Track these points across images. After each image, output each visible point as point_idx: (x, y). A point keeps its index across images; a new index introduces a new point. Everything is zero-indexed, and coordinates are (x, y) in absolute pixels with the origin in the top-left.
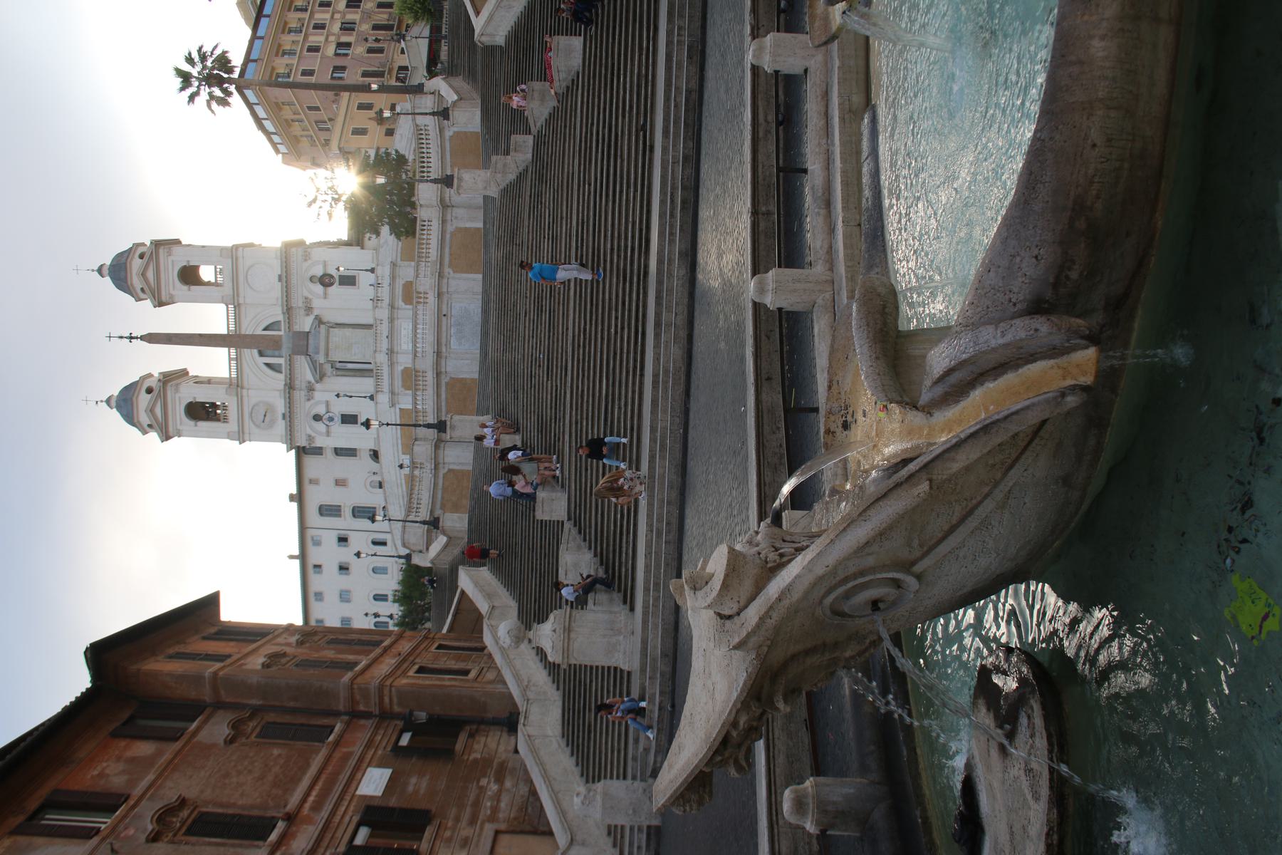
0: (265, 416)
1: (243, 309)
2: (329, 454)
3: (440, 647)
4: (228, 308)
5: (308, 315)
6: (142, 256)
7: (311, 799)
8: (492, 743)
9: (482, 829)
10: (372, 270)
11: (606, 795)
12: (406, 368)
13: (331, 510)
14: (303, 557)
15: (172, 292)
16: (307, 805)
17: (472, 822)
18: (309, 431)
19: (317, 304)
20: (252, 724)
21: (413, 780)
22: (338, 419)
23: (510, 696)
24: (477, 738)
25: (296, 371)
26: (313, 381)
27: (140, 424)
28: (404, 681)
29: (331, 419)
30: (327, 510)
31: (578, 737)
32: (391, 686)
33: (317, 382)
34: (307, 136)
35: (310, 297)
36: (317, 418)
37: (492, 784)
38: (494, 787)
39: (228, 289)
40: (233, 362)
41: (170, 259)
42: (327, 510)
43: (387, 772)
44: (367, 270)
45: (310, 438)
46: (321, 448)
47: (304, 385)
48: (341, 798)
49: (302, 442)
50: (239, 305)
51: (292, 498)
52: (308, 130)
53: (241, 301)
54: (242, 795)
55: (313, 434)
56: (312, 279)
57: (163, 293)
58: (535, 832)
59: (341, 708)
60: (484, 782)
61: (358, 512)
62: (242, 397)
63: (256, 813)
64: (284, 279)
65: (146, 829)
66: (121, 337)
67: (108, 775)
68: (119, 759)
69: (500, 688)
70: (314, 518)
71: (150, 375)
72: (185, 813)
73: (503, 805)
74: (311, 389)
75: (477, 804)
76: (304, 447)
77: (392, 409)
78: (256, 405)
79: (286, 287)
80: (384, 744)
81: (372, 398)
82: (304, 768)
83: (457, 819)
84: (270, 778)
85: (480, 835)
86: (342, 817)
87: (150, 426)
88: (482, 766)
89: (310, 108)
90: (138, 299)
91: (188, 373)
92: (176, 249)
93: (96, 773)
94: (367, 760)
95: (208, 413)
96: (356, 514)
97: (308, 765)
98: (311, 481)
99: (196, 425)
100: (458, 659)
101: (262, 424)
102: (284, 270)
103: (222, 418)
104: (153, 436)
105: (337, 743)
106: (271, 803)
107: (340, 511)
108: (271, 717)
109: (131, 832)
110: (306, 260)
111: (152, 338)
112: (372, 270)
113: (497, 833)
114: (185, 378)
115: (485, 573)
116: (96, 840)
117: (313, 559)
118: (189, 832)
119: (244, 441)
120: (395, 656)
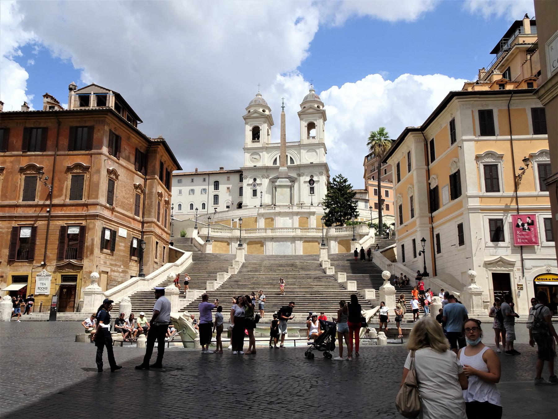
1: (298, 148)
2: (240, 185)
3: (164, 247)
5: (297, 175)
6: (318, 107)
7: (118, 214)
8: (134, 268)
9: (109, 267)
10: (312, 204)
11: (128, 305)
14: (197, 174)
16: (116, 213)
17: (111, 265)
20: (140, 191)
21: (123, 245)
23: (149, 274)
24: (135, 263)
27: (249, 108)
28: (154, 238)
29: (254, 185)
31: (138, 297)
32: (152, 235)
33: (270, 180)
34: (375, 169)
36: (255, 180)
37: (121, 269)
38: (121, 270)
39: (305, 141)
40: (276, 145)
41: (318, 118)
42: (217, 184)
43: (126, 237)
44: (312, 202)
45: (246, 178)
46: (242, 181)
48: (118, 223)
49: (244, 174)
50: (300, 147)
51: (221, 168)
54: (119, 193)
57: (304, 116)
58: (107, 284)
59: (145, 219)
60: (122, 267)
61: (216, 197)
63: (115, 198)
65: (110, 167)
66: (283, 103)
67: (125, 151)
68: (130, 153)
69: (151, 270)
70: (213, 179)
71: (270, 110)
72: (114, 177)
73: (115, 273)
75: (116, 265)
76: (242, 175)
77: (257, 214)
78: (260, 155)
80: (134, 234)
81: (261, 206)
82: (127, 210)
83: (112, 260)
84: (124, 200)
85: (107, 267)
86: (113, 225)
87: (249, 111)
88: (127, 266)
89: (385, 170)
90: (301, 105)
91: (272, 125)
92: (321, 121)
93: (126, 147)
94: (129, 229)
95: (256, 134)
96: (215, 196)
97: (128, 211)
98: (228, 177)
100: (160, 254)
103: (254, 141)
104: (245, 113)
105: (134, 219)
106: (117, 202)
107: (217, 190)
108: (142, 196)
109: (110, 163)
110: (320, 173)
111: (283, 116)
112: (312, 204)
113: (108, 272)
114: (269, 124)
115: (190, 261)
116: (108, 154)
117: (196, 179)
118: (110, 180)
119: (244, 150)
120: (161, 233)
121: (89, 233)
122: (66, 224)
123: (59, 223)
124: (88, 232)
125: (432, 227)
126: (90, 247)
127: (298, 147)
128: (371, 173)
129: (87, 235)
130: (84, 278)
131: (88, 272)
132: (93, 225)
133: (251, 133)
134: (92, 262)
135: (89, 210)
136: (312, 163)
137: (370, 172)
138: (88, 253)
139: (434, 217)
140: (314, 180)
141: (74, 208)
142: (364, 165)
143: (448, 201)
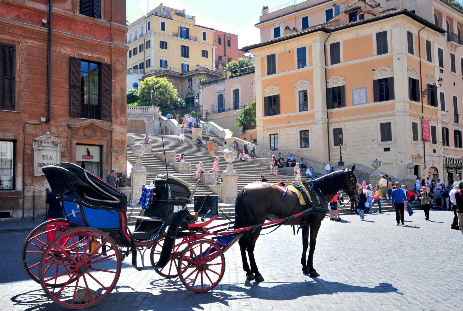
121: (118, 78)
122: (78, 54)
123: (65, 50)
124: (115, 77)
125: (328, 121)
126: (120, 102)
129: (113, 81)
130: (116, 152)
131: (119, 141)
132: (121, 66)
134: (124, 126)
135: (113, 40)
138: (118, 112)
139: (331, 113)
141: (87, 28)
143: (365, 102)
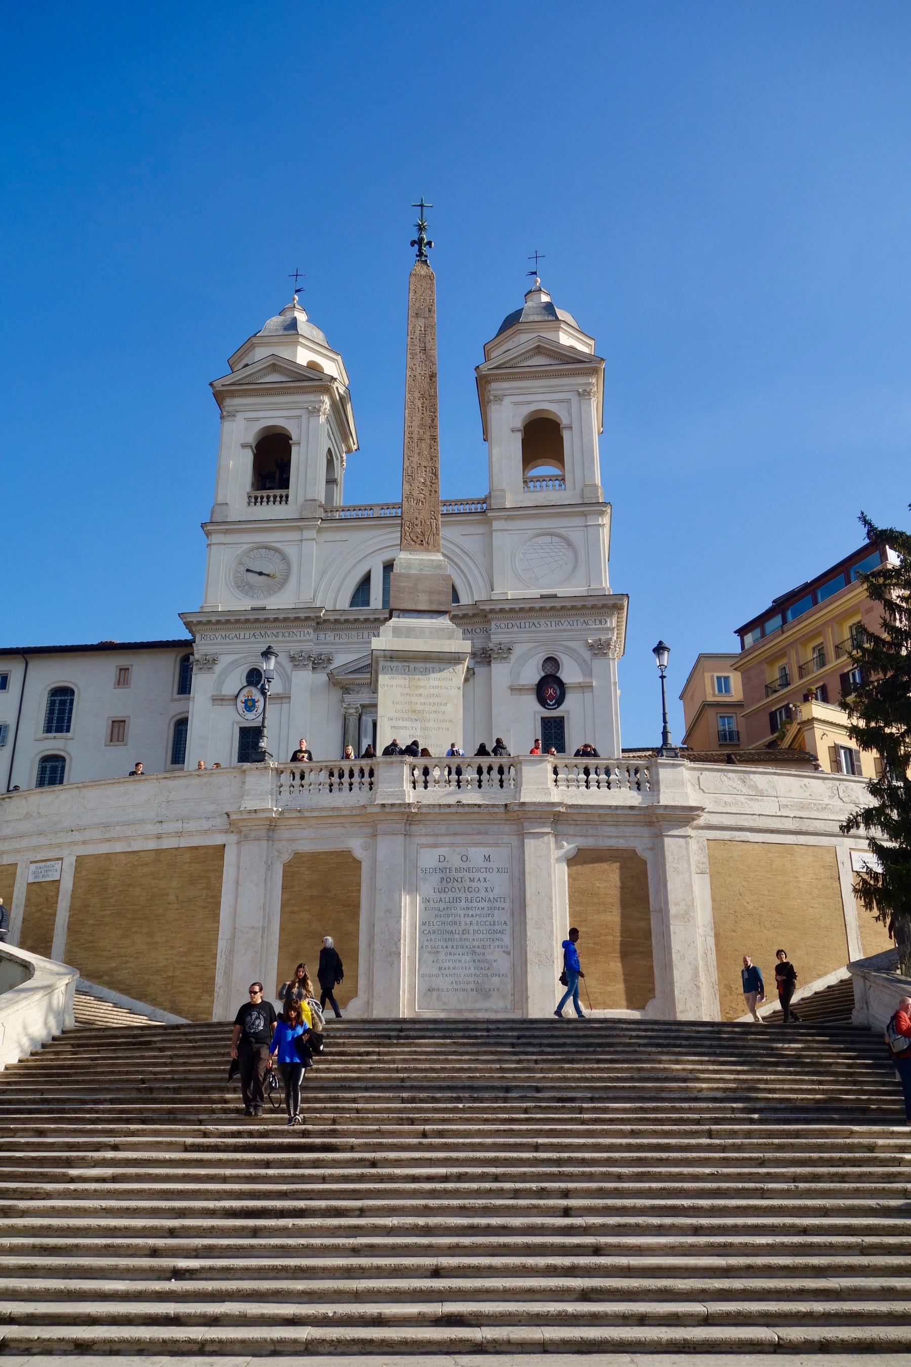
0: (261, 574)
1: (480, 529)
4: (484, 501)
12: (358, 863)
13: (61, 711)
15: (507, 401)
18: (224, 661)
19: (500, 671)
22: (252, 719)
25: (354, 633)
26: (332, 667)
30: (63, 703)
33: (330, 675)
35: (513, 657)
42: (63, 703)
45: (210, 662)
47: (324, 649)
50: (489, 522)
52: (801, 677)
53: (496, 525)
55: (218, 668)
56: (552, 662)
57: (505, 385)
62: (300, 529)
64: (548, 604)
74: (318, 662)
77: (221, 822)
78: (284, 558)
79: (531, 609)
96: (49, 765)
98: (124, 671)
99: (244, 446)
101: (243, 569)
102: (568, 604)
107: (59, 730)
110: (591, 647)
119: (208, 534)
127: (478, 522)
128: (767, 696)
133: (247, 459)
136: (555, 596)
137: (763, 691)
140: (565, 680)
142: (681, 697)
